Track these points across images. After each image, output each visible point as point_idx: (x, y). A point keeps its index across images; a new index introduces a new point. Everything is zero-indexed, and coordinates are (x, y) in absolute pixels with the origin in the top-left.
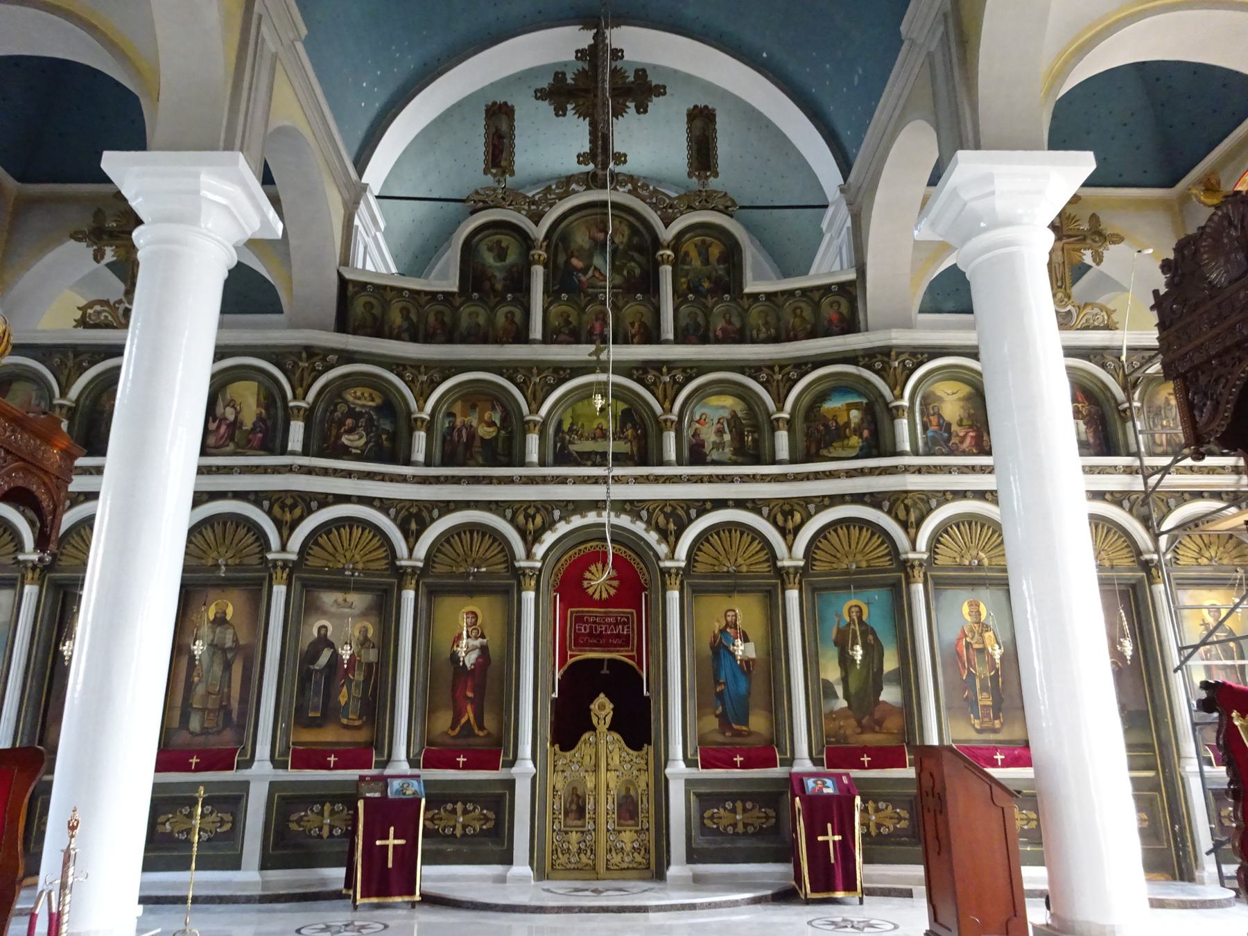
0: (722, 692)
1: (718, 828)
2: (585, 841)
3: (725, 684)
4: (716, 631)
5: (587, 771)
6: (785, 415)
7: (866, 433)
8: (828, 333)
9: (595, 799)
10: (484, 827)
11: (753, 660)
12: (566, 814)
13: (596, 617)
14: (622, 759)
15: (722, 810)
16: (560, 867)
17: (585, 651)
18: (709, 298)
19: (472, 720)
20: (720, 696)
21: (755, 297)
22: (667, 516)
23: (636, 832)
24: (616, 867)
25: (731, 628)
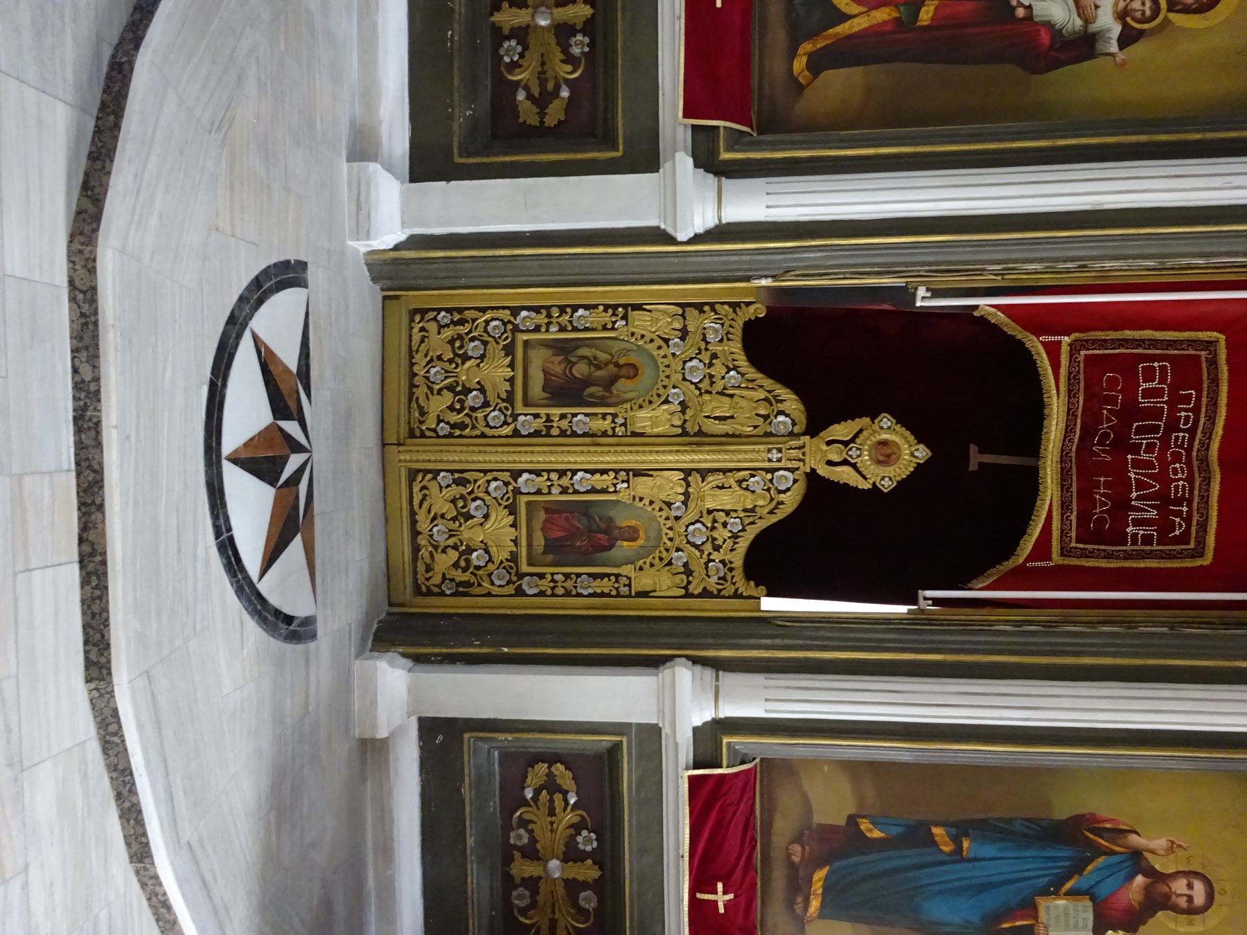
0: (932, 842)
1: (525, 803)
2: (486, 404)
4: (1133, 839)
5: (684, 406)
9: (605, 434)
10: (521, 96)
12: (561, 348)
13: (1192, 431)
14: (721, 517)
15: (570, 817)
16: (417, 336)
17: (1071, 393)
19: (843, 29)
23: (514, 558)
24: (417, 498)
25: (1147, 889)
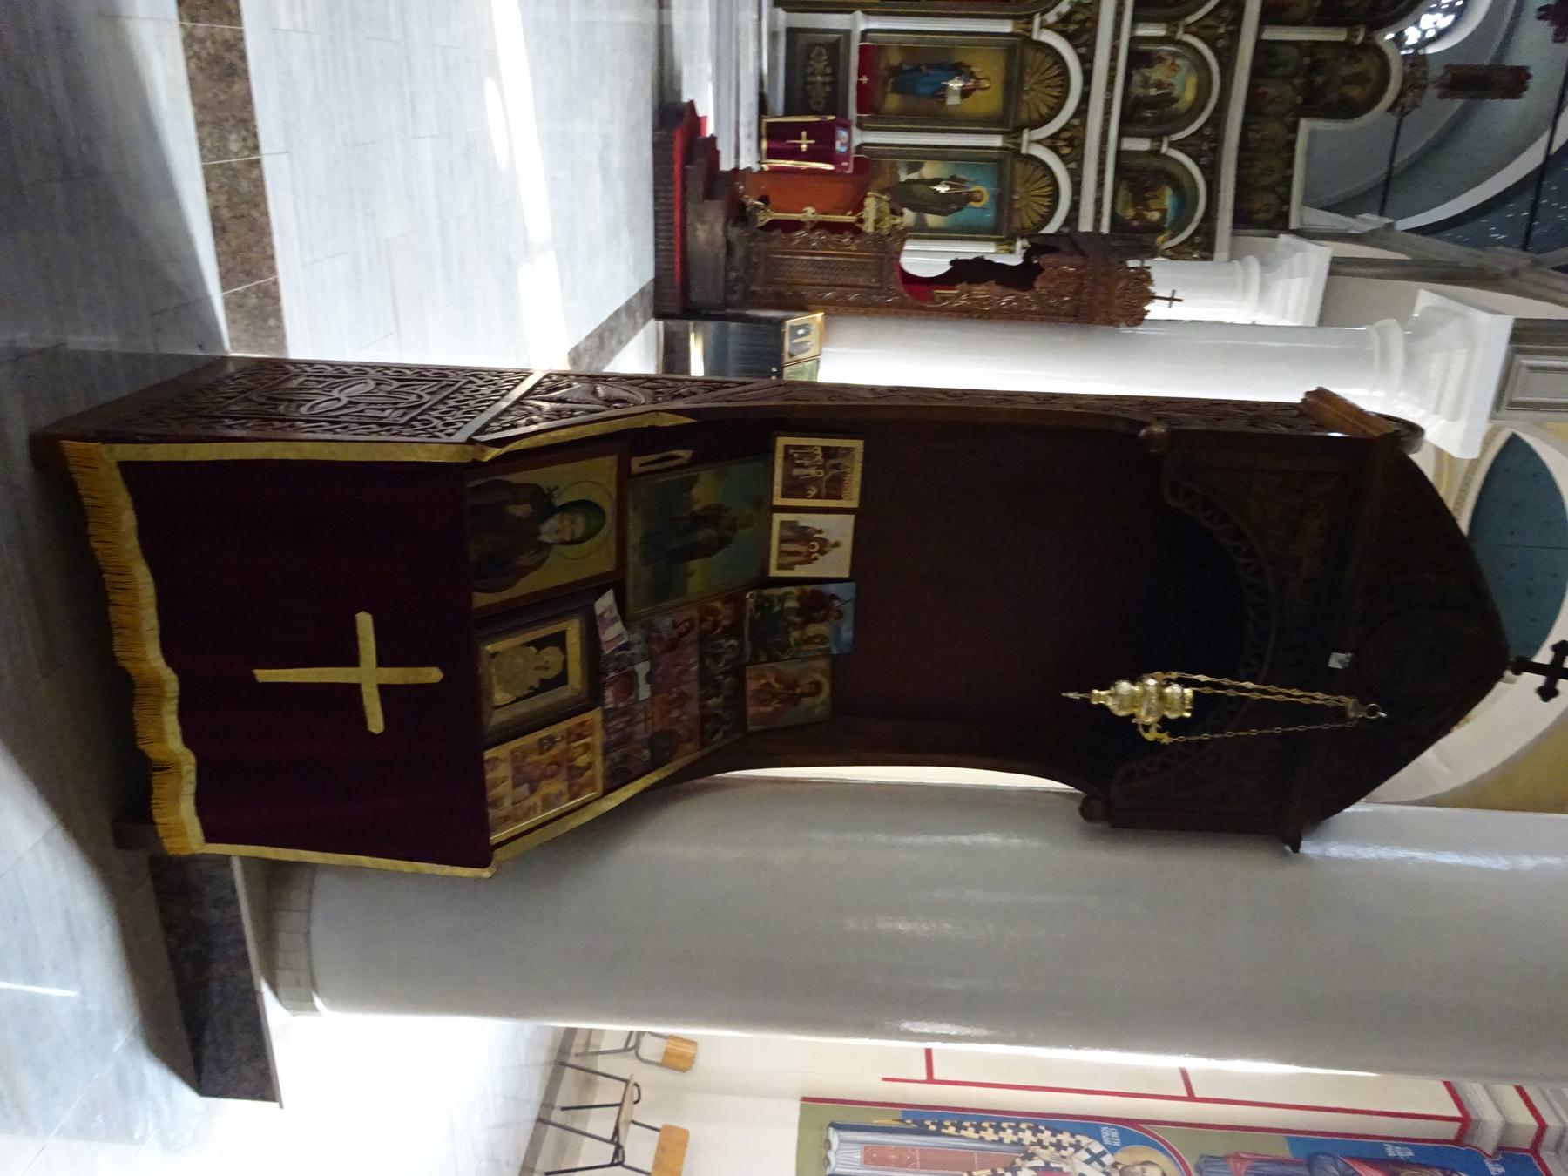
3: (927, 75)
4: (973, 69)
6: (1164, 149)
7: (1136, 223)
8: (1239, 197)
11: (945, 101)
15: (825, 63)
18: (1303, 80)
20: (917, 69)
21: (1294, 129)
22: (1082, 22)
